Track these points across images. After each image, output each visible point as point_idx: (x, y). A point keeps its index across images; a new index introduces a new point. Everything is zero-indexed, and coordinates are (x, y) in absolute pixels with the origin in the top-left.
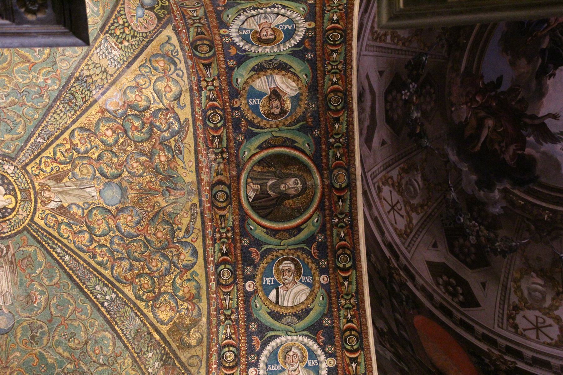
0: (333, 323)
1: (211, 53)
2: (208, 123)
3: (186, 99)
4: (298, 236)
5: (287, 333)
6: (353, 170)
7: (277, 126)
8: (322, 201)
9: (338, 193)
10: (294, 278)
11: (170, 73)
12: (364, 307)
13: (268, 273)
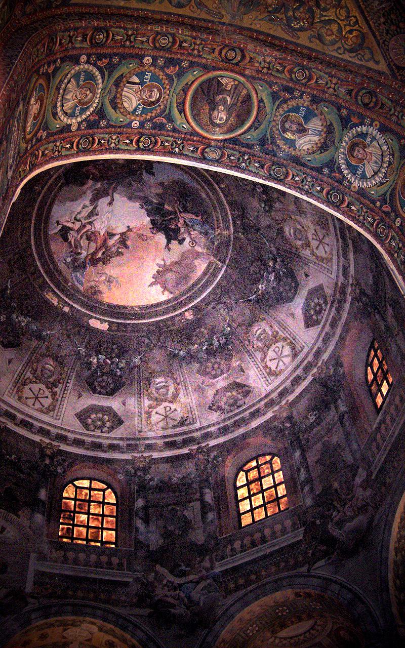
0: (101, 128)
1: (360, 103)
2: (298, 68)
3: (316, 45)
4: (176, 109)
5: (104, 89)
6: (216, 165)
7: (274, 120)
8: (198, 135)
9: (201, 149)
10: (144, 99)
11: (343, 41)
12: (106, 153)
13: (154, 78)
